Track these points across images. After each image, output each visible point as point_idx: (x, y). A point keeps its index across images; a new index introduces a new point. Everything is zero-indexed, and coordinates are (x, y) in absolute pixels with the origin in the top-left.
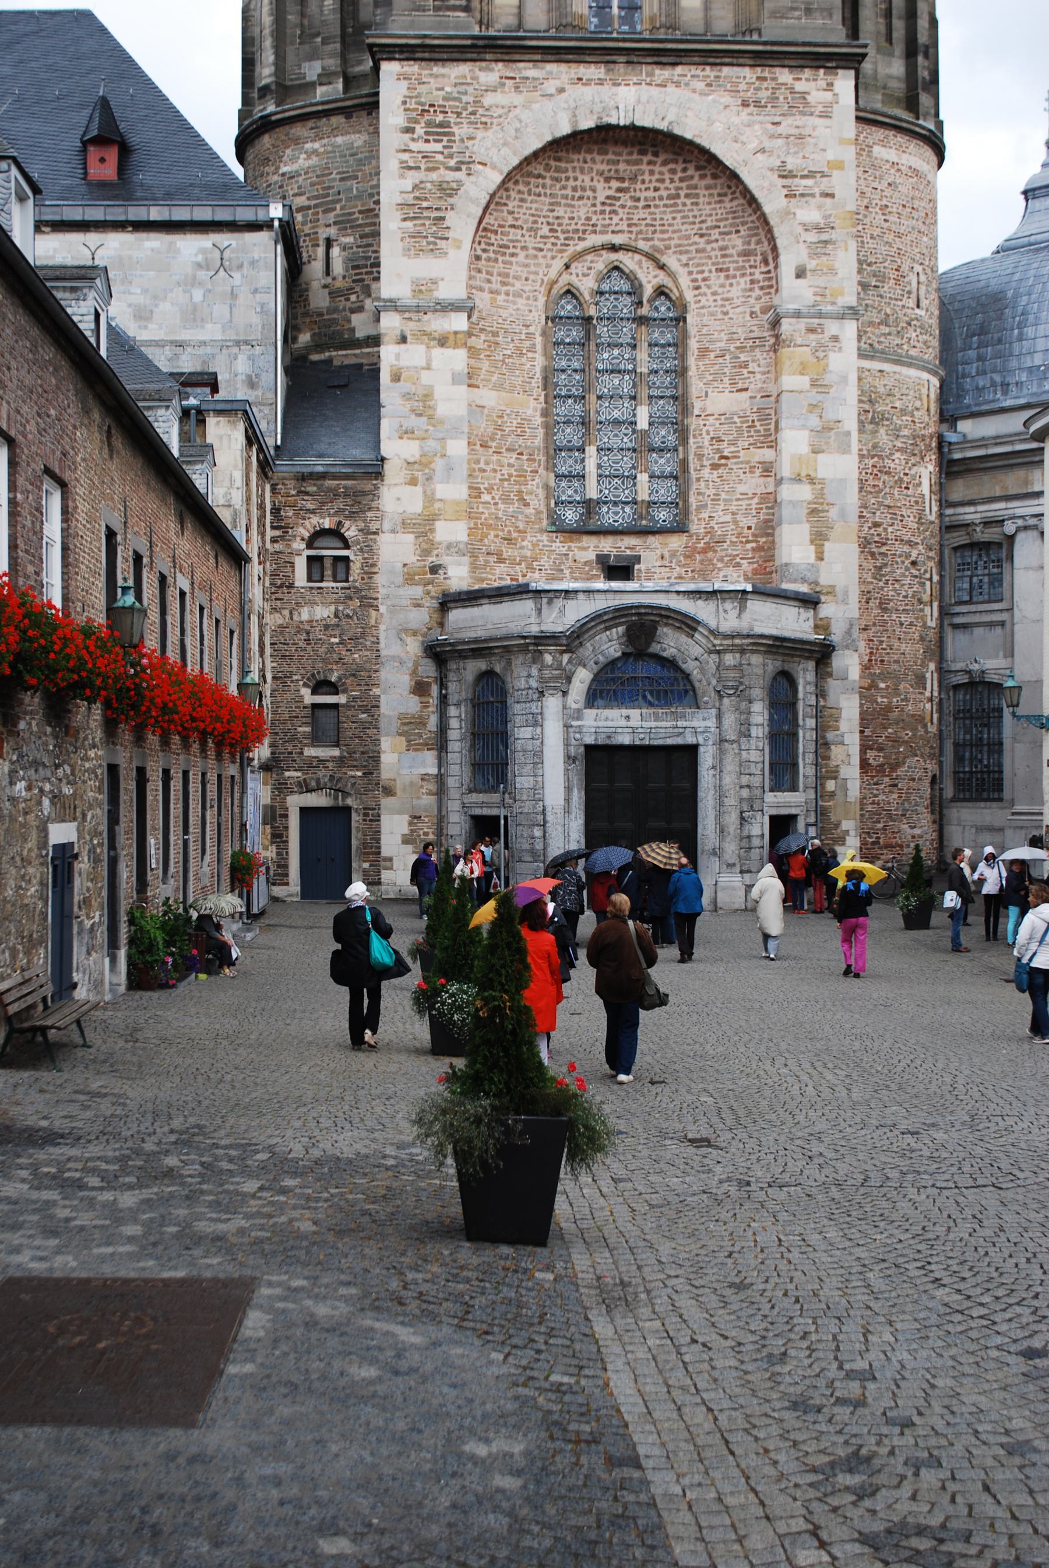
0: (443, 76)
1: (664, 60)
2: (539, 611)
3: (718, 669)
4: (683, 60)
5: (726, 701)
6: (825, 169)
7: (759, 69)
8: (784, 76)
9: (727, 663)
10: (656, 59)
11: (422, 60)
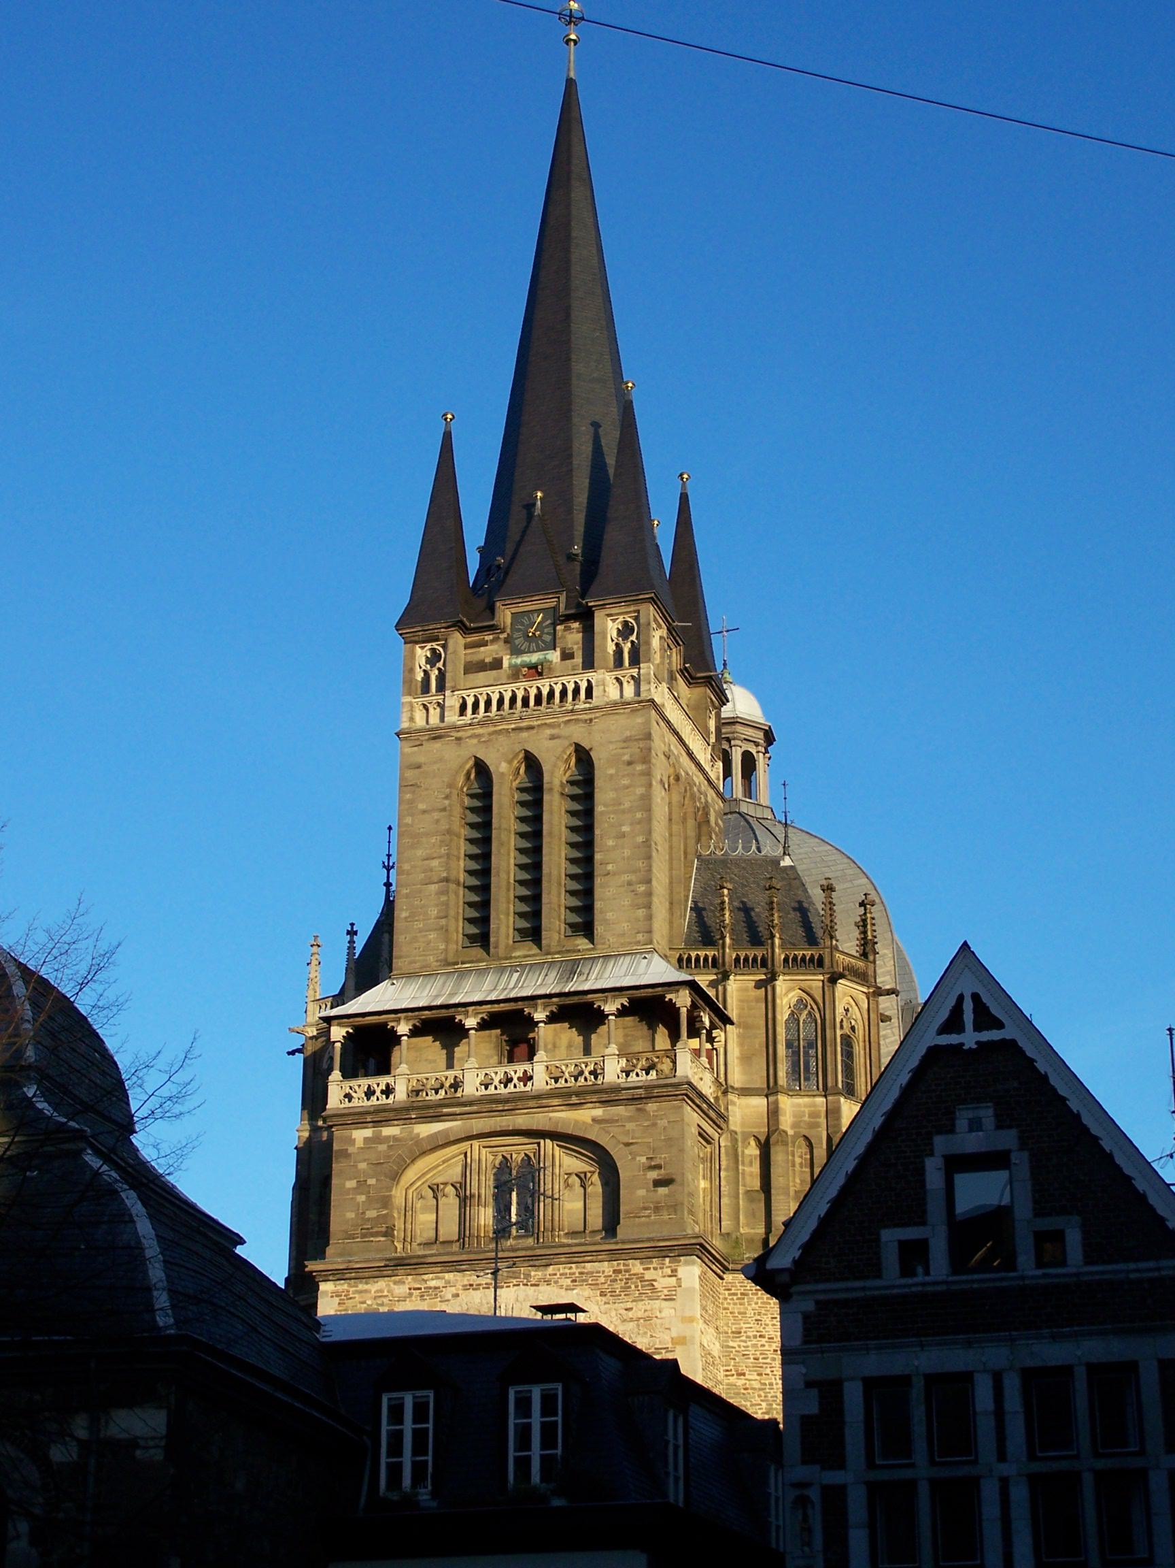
0: (366, 1291)
1: (537, 1263)
4: (552, 1262)
6: (670, 1345)
7: (615, 1263)
8: (636, 1267)
10: (531, 1263)
11: (350, 1279)
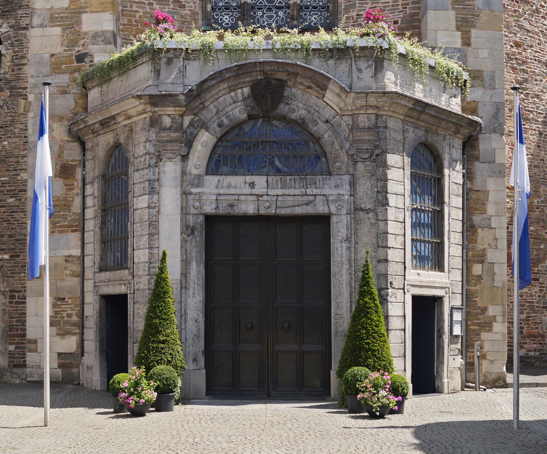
2: (157, 73)
3: (351, 130)
5: (360, 166)
9: (361, 125)
